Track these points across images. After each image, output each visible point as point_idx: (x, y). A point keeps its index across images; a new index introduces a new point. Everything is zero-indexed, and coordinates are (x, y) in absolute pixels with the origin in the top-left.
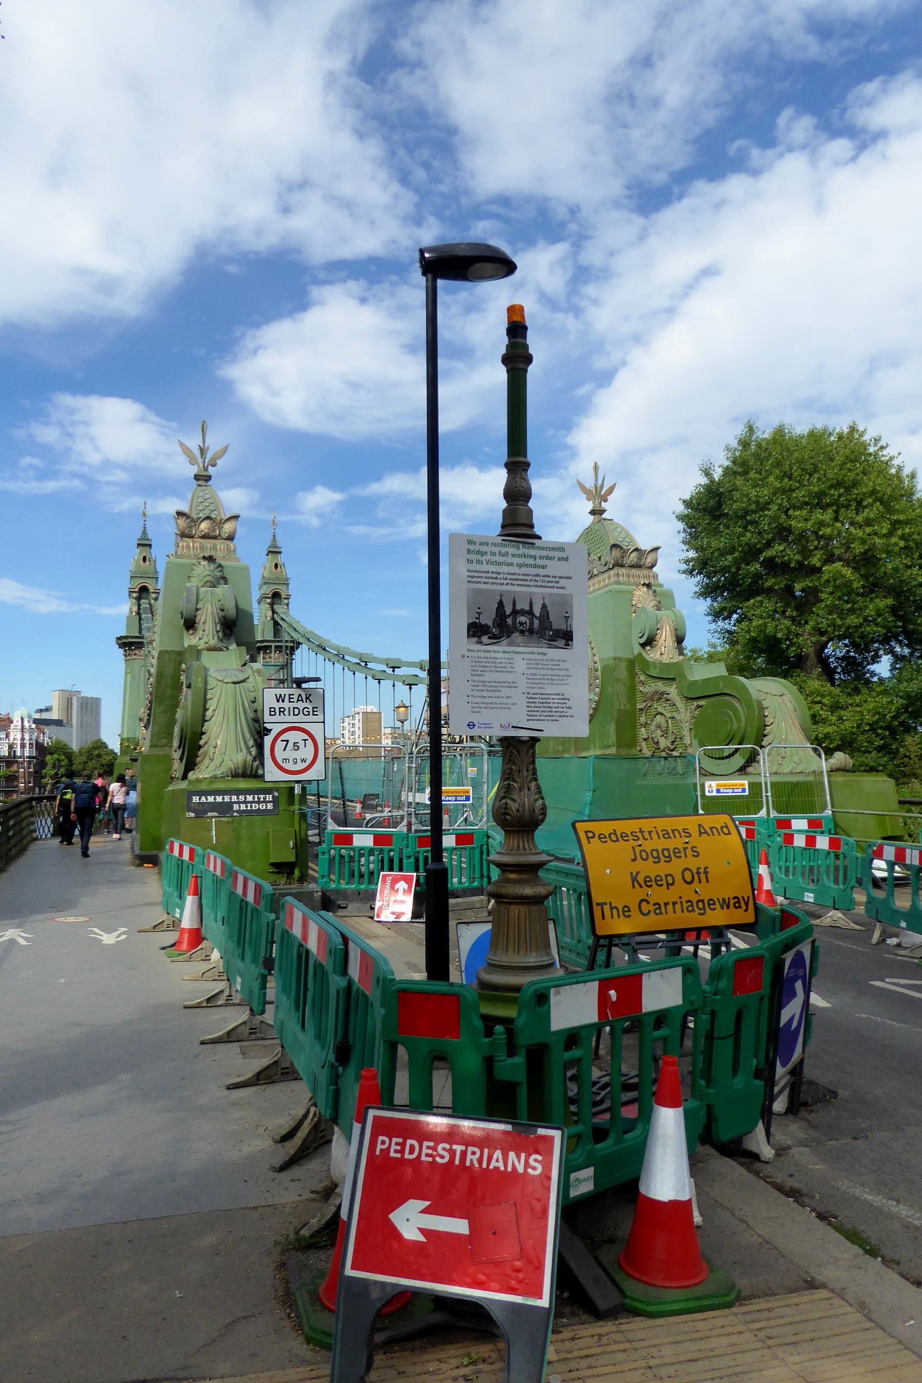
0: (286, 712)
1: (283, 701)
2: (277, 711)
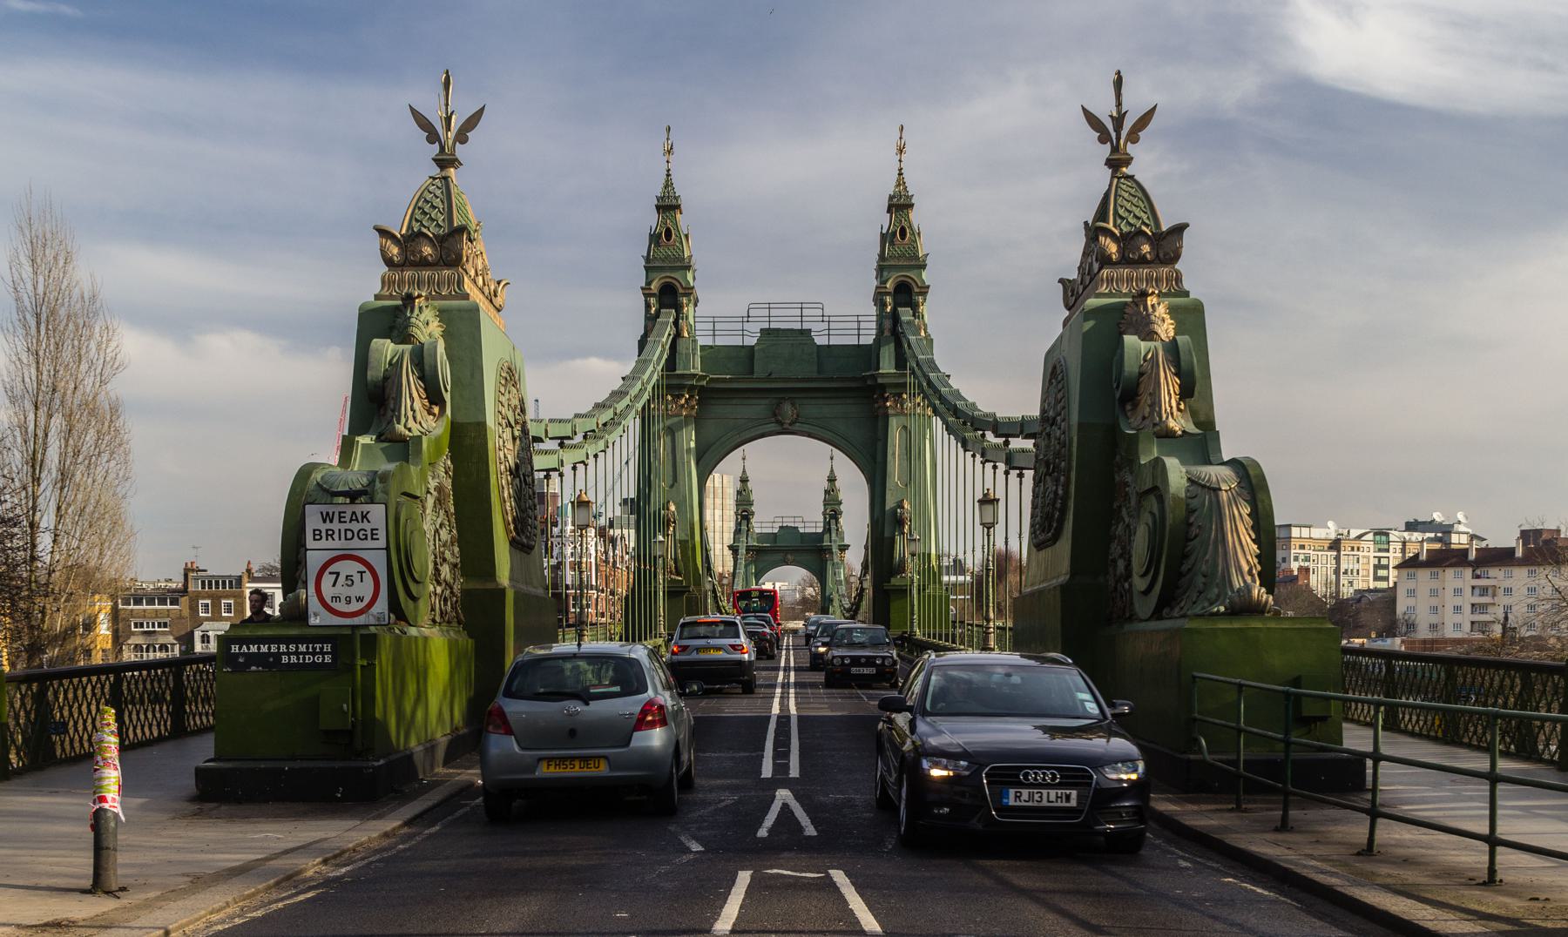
1: (331, 521)
2: (324, 535)
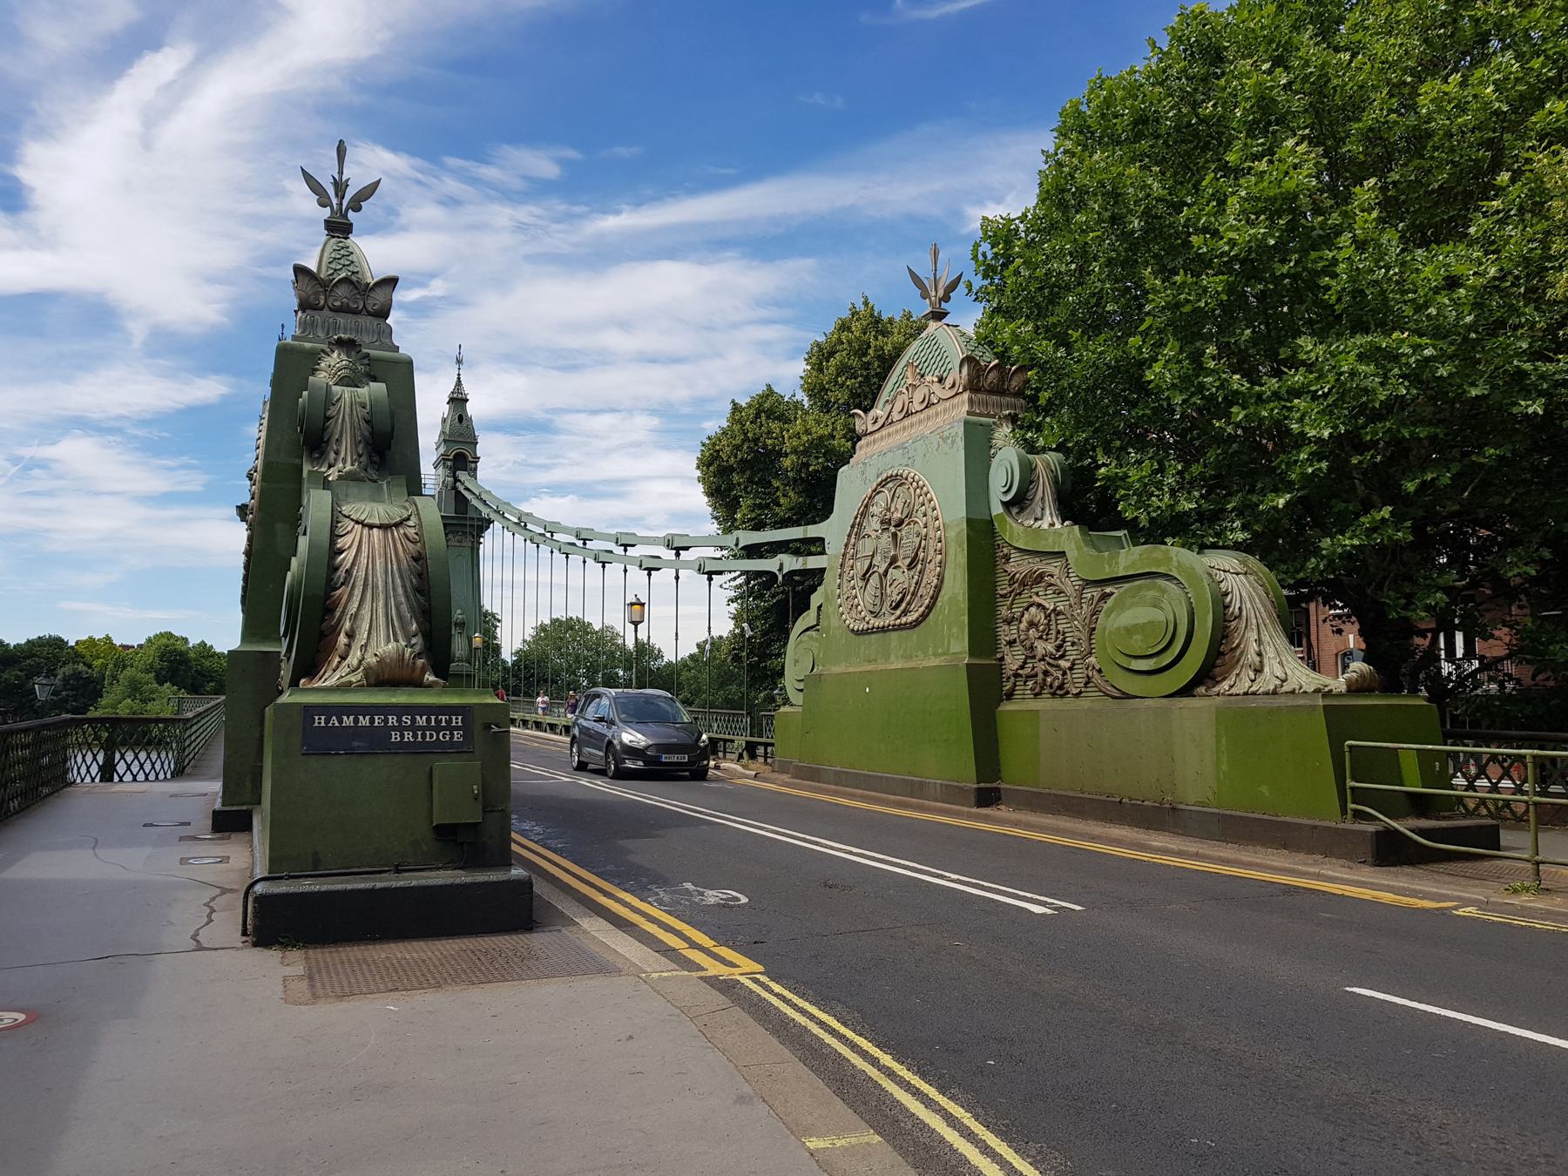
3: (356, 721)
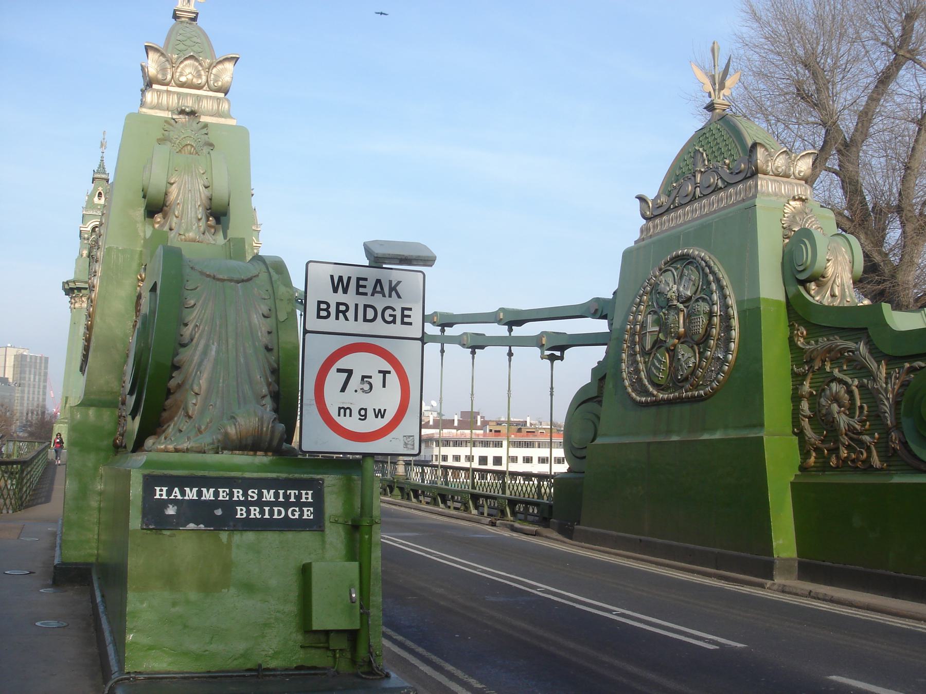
0: (351, 314)
1: (345, 291)
2: (333, 310)
3: (200, 494)
